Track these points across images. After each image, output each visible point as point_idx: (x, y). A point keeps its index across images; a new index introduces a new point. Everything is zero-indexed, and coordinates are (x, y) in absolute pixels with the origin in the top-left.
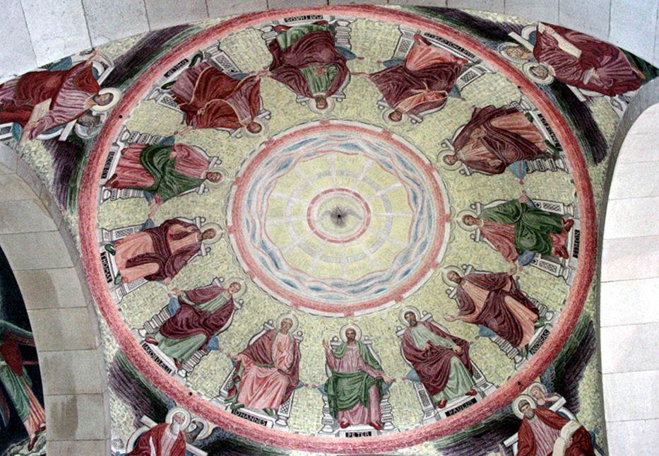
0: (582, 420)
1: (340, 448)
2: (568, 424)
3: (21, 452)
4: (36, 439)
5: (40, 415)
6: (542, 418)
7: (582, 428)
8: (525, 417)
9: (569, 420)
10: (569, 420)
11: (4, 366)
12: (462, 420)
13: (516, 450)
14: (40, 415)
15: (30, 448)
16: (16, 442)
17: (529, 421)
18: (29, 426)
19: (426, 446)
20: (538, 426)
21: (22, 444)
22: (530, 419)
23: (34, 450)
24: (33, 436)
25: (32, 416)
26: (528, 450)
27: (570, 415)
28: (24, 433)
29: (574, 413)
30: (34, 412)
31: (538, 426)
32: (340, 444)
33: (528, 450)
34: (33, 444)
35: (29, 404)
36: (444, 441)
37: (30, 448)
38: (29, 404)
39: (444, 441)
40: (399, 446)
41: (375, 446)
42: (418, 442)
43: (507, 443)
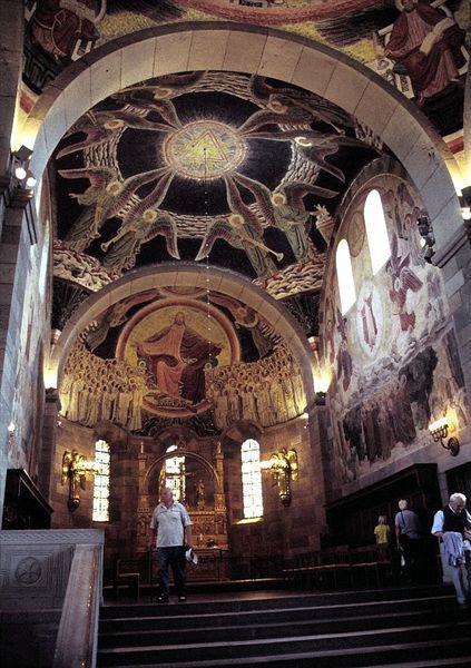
0: (457, 18)
1: (232, 14)
2: (444, 21)
6: (421, 13)
7: (457, 25)
8: (405, 10)
9: (444, 15)
10: (444, 15)
12: (346, 6)
13: (387, 40)
17: (408, 15)
19: (308, 25)
20: (415, 21)
22: (409, 12)
26: (399, 40)
27: (448, 13)
29: (453, 12)
31: (415, 21)
32: (232, 10)
33: (399, 40)
36: (324, 23)
39: (324, 23)
40: (284, 21)
41: (263, 18)
42: (302, 20)
43: (381, 32)
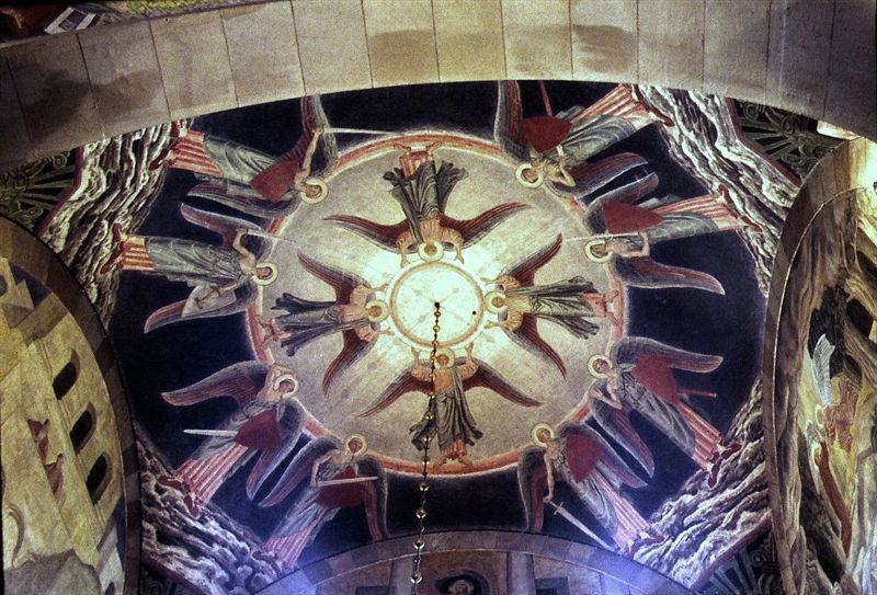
3: (678, 141)
4: (656, 111)
5: (621, 100)
11: (565, 151)
14: (621, 100)
15: (670, 123)
16: (666, 148)
18: (640, 121)
21: (667, 137)
23: (671, 116)
24: (653, 116)
25: (625, 113)
28: (651, 129)
30: (619, 108)
34: (664, 117)
35: (608, 116)
37: (670, 123)
38: (608, 116)
